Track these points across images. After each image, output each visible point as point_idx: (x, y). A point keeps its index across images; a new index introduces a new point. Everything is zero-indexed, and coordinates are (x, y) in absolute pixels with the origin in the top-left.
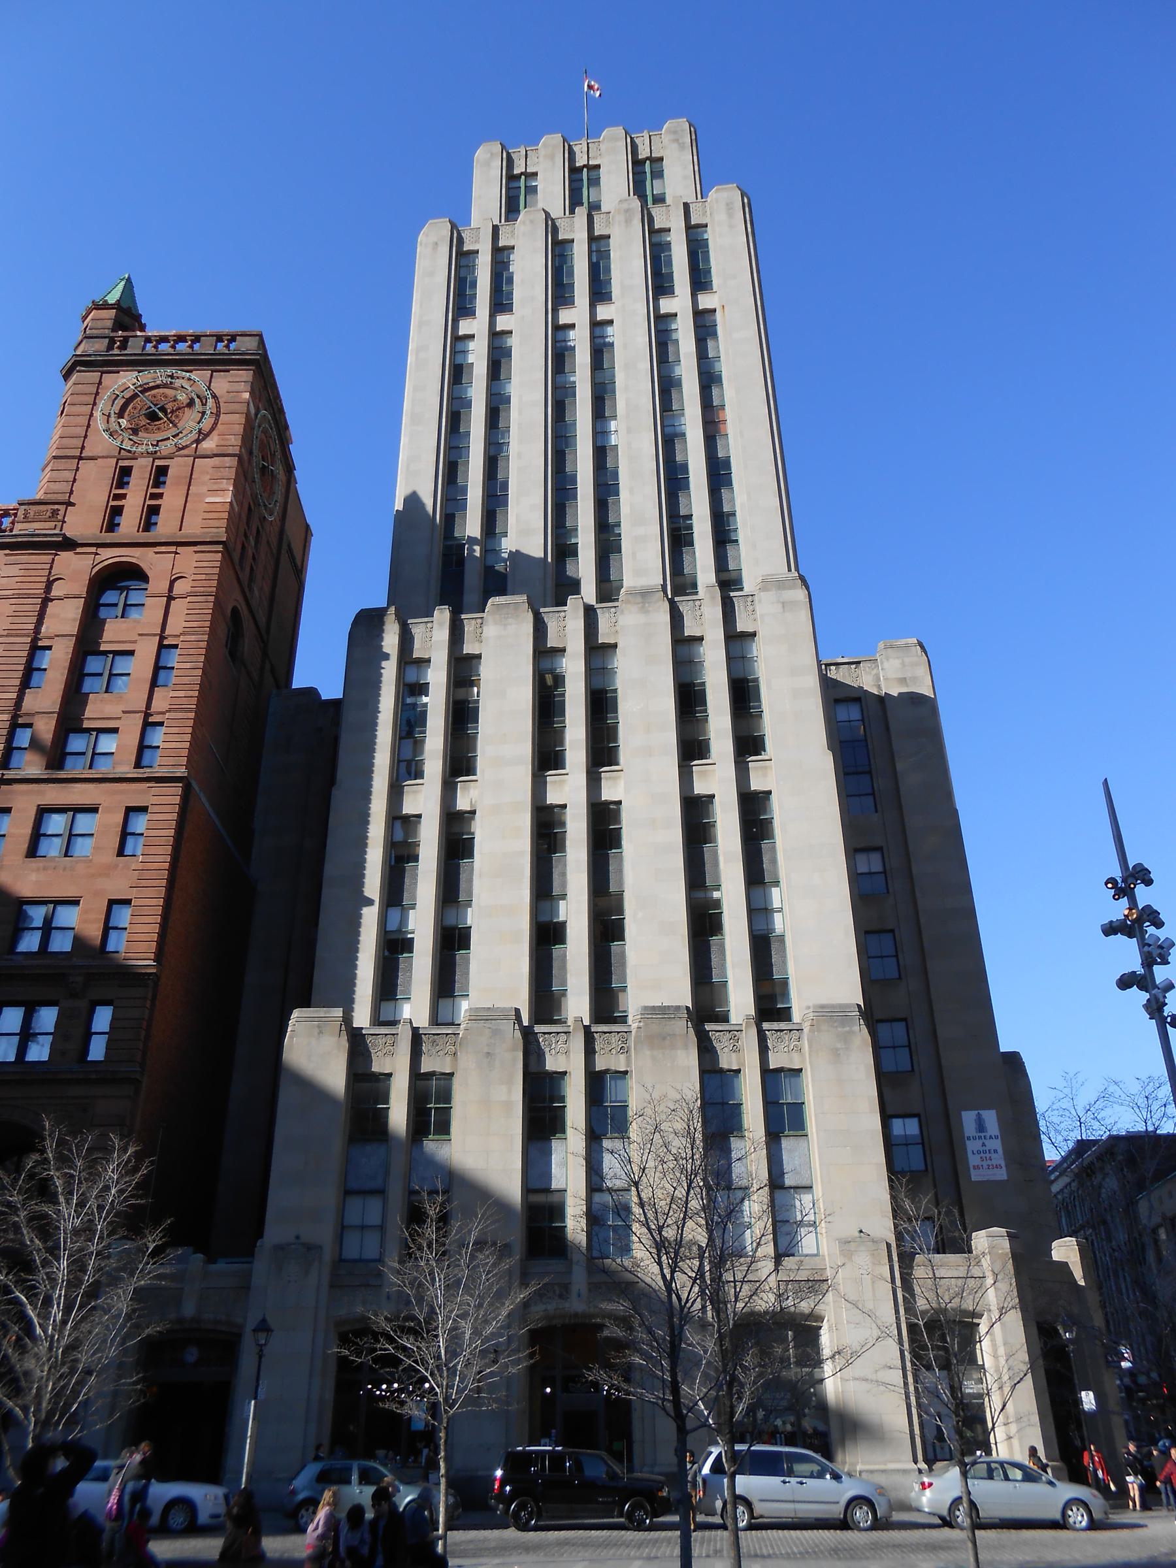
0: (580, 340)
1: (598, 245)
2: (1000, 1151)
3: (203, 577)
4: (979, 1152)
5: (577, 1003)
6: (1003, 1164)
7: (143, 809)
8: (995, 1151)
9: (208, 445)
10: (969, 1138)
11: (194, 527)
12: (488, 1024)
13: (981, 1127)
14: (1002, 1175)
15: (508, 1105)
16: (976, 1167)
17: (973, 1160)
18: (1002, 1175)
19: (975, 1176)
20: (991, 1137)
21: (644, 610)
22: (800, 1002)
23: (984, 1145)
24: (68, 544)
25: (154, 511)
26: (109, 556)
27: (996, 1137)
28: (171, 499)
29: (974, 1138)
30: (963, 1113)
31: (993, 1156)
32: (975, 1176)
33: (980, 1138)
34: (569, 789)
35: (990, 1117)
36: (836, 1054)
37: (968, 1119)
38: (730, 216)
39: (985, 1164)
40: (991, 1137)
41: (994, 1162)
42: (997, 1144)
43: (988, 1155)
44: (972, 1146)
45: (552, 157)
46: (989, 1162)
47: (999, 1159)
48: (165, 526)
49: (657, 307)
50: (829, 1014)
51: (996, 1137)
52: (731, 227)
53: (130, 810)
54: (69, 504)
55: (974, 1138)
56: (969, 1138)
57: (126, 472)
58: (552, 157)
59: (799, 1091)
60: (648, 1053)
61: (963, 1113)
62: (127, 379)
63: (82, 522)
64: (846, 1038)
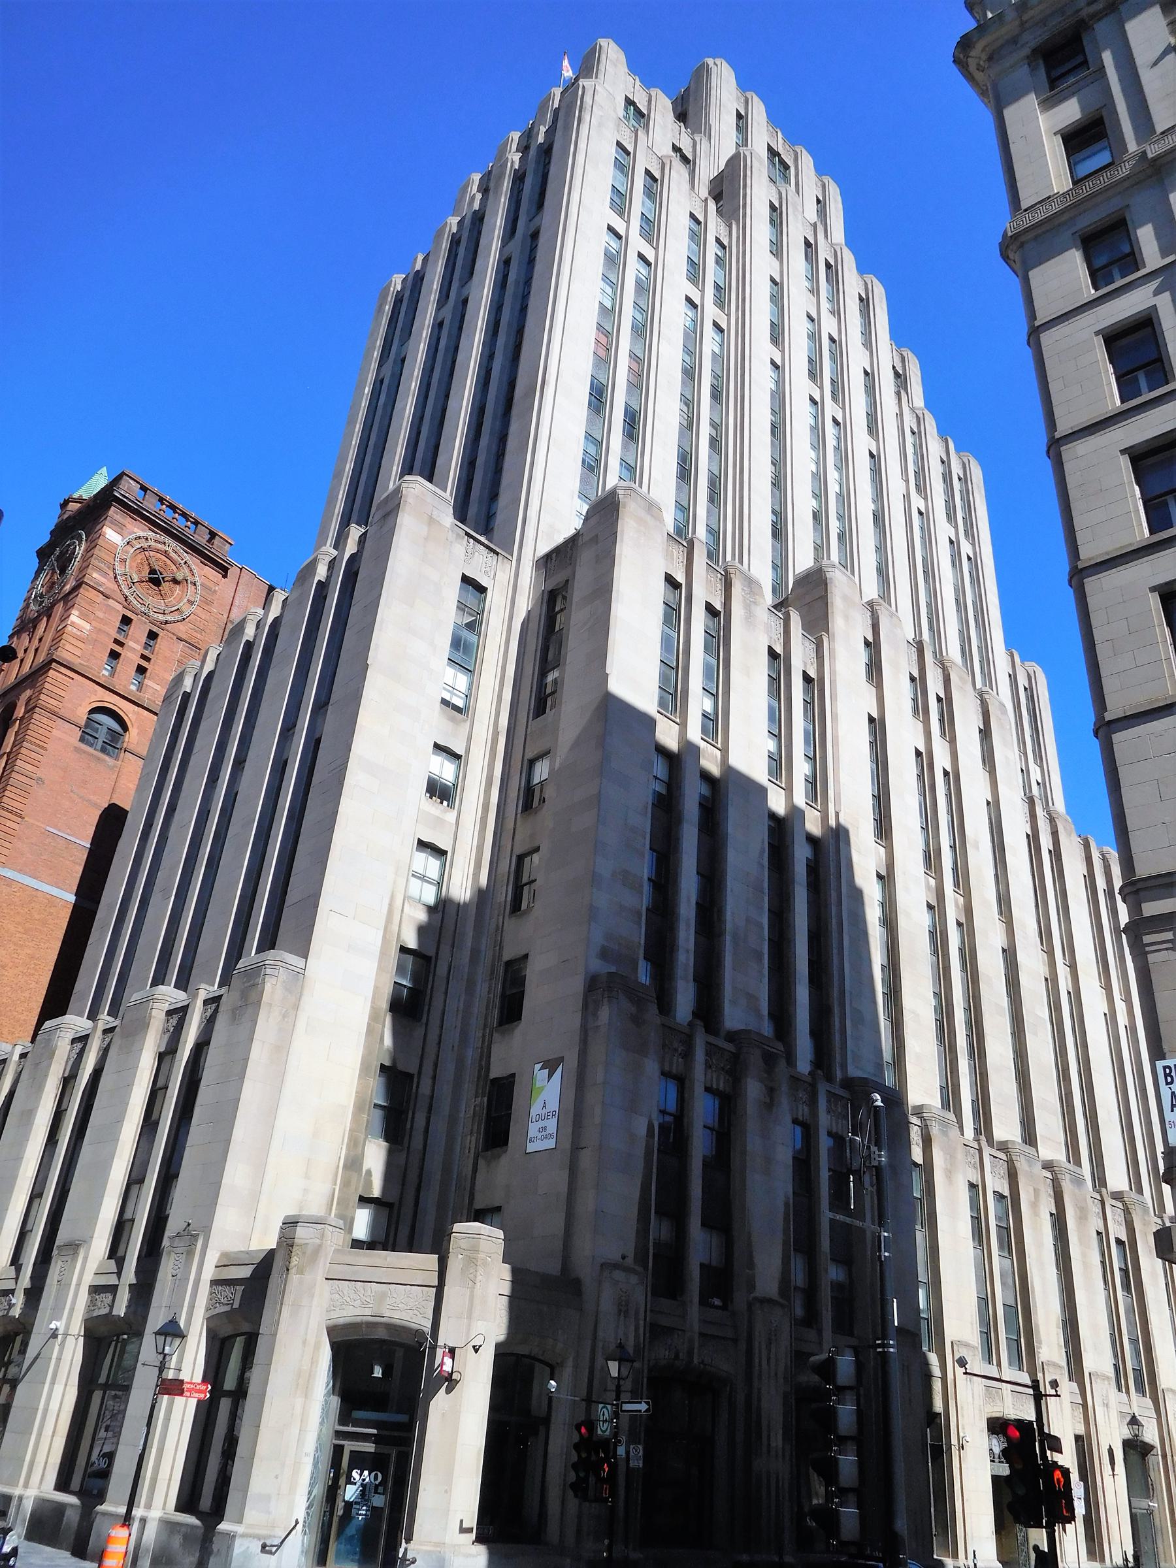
17: (533, 1130)
47: (552, 1125)
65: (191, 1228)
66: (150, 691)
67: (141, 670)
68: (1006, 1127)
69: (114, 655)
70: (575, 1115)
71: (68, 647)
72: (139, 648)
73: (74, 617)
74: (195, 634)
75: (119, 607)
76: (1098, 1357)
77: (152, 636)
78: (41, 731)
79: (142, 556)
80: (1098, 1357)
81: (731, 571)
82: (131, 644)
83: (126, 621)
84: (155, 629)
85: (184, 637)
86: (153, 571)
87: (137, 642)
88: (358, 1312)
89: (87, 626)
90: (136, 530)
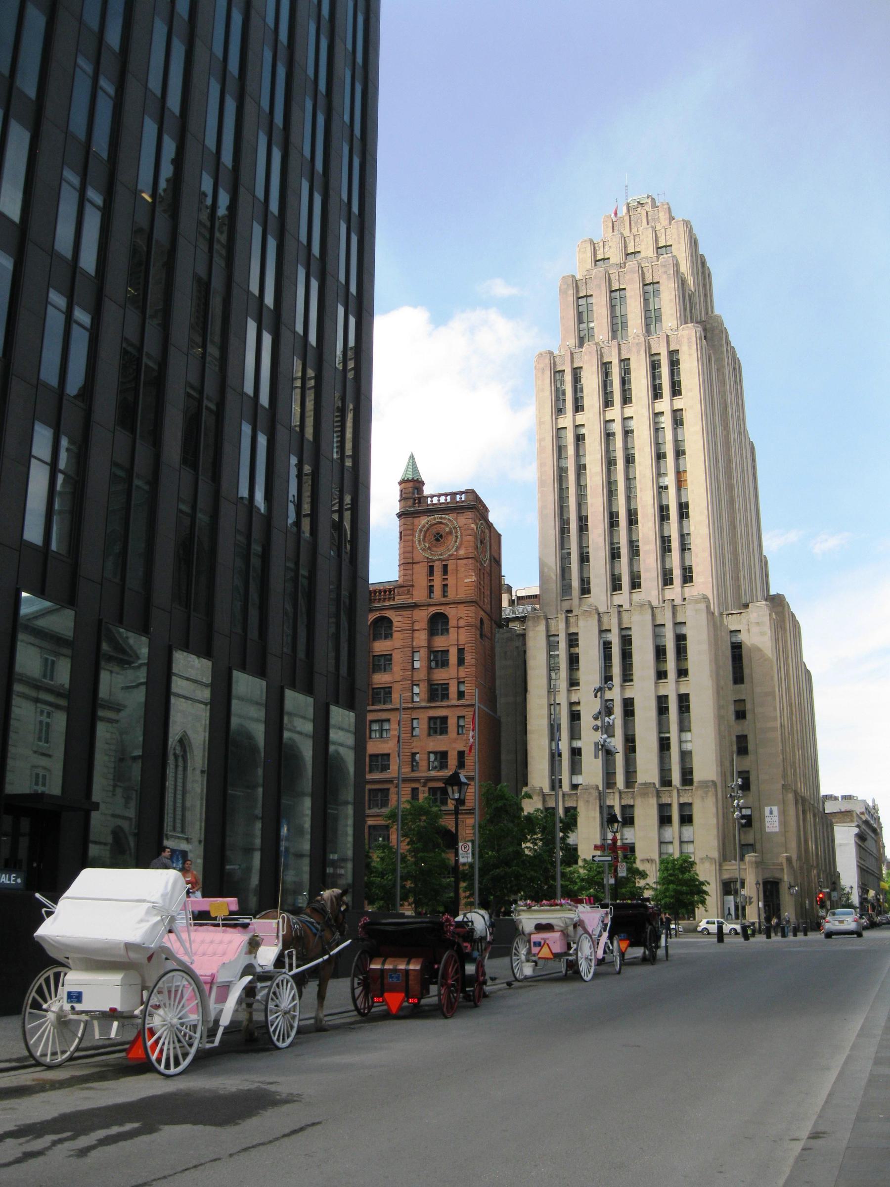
0: (617, 428)
1: (625, 363)
5: (620, 780)
7: (463, 717)
9: (462, 552)
11: (462, 595)
13: (771, 813)
14: (777, 830)
15: (594, 818)
17: (767, 824)
19: (767, 830)
22: (697, 776)
24: (415, 606)
25: (445, 586)
26: (433, 610)
28: (451, 581)
32: (767, 830)
35: (775, 809)
36: (703, 798)
37: (767, 810)
38: (690, 347)
42: (776, 819)
44: (767, 819)
45: (599, 286)
47: (777, 824)
48: (452, 595)
49: (653, 409)
50: (705, 785)
52: (690, 355)
53: (459, 717)
54: (412, 586)
57: (431, 568)
58: (599, 286)
59: (691, 810)
62: (424, 521)
63: (419, 595)
64: (706, 793)
70: (784, 823)
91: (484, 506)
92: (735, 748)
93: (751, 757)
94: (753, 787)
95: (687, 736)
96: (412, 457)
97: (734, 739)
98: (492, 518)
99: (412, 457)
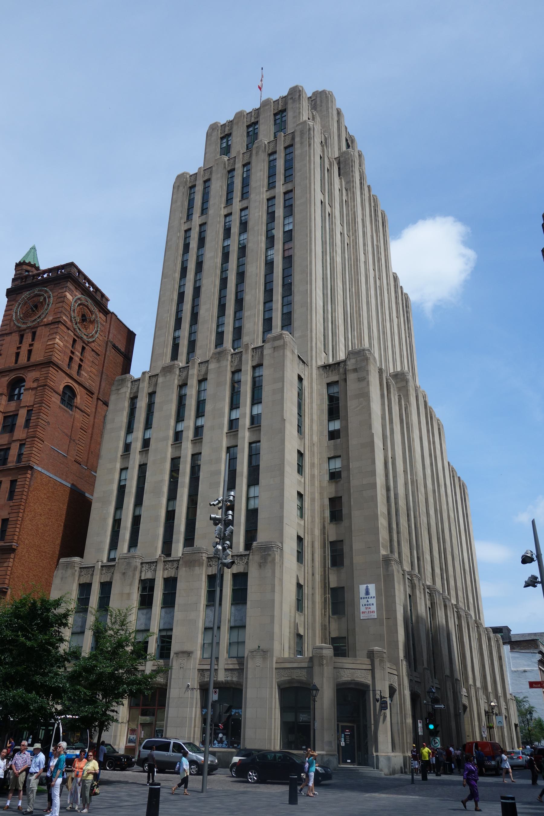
2: (375, 604)
3: (43, 378)
4: (365, 605)
6: (375, 611)
8: (373, 604)
10: (361, 598)
12: (126, 560)
13: (367, 593)
16: (363, 613)
17: (362, 609)
18: (375, 615)
19: (362, 616)
20: (371, 597)
21: (218, 361)
23: (368, 601)
26: (13, 376)
27: (374, 597)
29: (364, 598)
30: (360, 586)
31: (371, 606)
32: (362, 616)
33: (366, 598)
34: (187, 449)
35: (372, 588)
37: (362, 588)
39: (367, 611)
40: (371, 597)
41: (371, 610)
42: (373, 601)
43: (369, 606)
44: (363, 602)
46: (369, 610)
48: (32, 360)
51: (374, 597)
55: (364, 598)
56: (361, 598)
60: (184, 569)
61: (360, 586)
62: (26, 295)
65: (260, 648)
66: (83, 377)
67: (80, 366)
68: (454, 602)
69: (71, 359)
71: (56, 355)
72: (79, 355)
73: (57, 340)
74: (98, 348)
75: (72, 334)
76: (478, 684)
77: (83, 348)
78: (48, 398)
79: (79, 308)
80: (478, 684)
81: (389, 381)
82: (77, 353)
83: (74, 341)
84: (84, 345)
85: (94, 349)
86: (83, 316)
87: (78, 352)
88: (346, 679)
89: (62, 344)
90: (77, 294)
91: (103, 295)
92: (327, 514)
93: (345, 523)
94: (346, 561)
95: (254, 491)
96: (34, 248)
97: (327, 502)
98: (111, 307)
99: (34, 248)
